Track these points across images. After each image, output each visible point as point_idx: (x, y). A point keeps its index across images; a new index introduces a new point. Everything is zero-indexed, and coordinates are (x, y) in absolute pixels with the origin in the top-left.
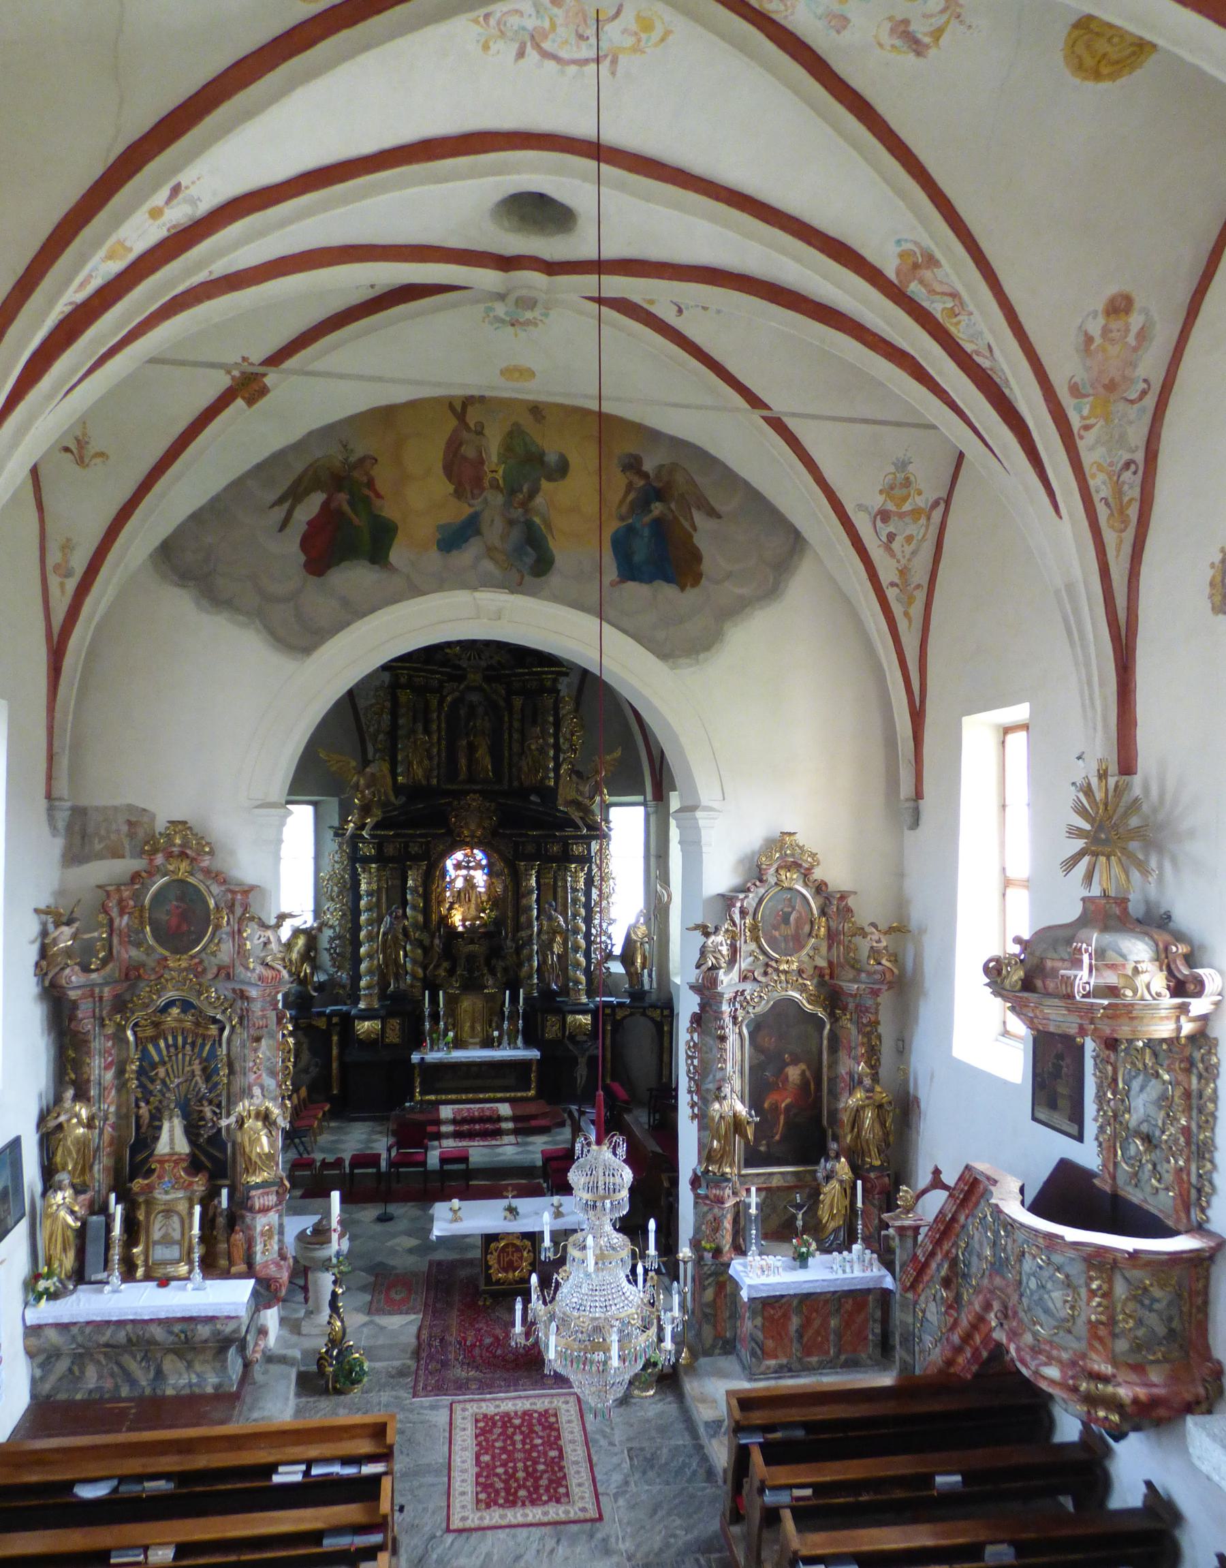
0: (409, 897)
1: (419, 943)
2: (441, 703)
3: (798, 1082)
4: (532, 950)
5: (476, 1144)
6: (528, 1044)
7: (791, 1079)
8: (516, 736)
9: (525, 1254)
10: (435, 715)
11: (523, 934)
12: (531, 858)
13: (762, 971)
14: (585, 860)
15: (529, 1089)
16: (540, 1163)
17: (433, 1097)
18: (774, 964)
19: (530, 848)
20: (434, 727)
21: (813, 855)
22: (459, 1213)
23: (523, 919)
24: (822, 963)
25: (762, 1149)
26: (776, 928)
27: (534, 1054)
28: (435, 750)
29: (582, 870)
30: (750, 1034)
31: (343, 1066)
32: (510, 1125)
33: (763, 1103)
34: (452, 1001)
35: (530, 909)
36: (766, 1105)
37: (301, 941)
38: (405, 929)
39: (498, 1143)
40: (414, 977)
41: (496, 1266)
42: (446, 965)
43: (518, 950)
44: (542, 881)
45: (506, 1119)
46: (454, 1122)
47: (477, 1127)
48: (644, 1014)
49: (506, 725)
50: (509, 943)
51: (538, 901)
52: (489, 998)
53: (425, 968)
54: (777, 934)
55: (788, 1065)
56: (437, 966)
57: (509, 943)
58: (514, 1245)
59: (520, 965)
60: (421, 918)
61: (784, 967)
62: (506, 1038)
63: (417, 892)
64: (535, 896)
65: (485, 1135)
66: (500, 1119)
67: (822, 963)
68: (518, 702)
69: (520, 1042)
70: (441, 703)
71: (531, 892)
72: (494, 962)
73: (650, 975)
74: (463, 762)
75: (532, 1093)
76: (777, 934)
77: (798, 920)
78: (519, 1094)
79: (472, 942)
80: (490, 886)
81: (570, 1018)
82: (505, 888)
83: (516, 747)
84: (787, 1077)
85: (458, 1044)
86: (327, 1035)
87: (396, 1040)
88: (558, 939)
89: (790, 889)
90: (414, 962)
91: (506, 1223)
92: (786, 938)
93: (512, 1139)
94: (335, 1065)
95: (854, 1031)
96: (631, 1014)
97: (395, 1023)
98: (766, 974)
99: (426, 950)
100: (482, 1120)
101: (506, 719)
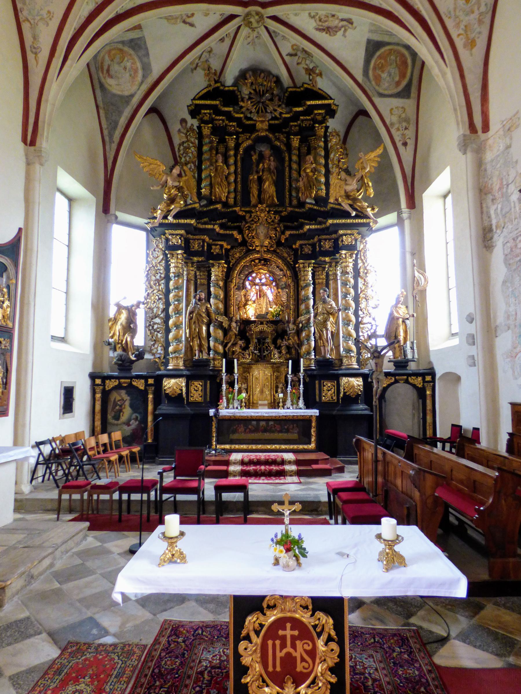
0: (212, 289)
1: (220, 326)
2: (237, 146)
4: (310, 332)
5: (261, 481)
6: (308, 406)
8: (295, 166)
9: (320, 643)
10: (232, 153)
11: (302, 318)
12: (308, 257)
14: (351, 248)
15: (310, 443)
16: (324, 498)
17: (227, 447)
19: (307, 250)
20: (232, 161)
22: (181, 545)
23: (303, 307)
27: (315, 412)
28: (232, 179)
29: (351, 257)
31: (155, 417)
32: (294, 468)
34: (246, 369)
35: (308, 298)
37: (124, 316)
38: (207, 309)
39: (282, 481)
40: (216, 352)
41: (258, 668)
42: (240, 342)
43: (298, 332)
44: (317, 281)
45: (290, 463)
46: (242, 463)
47: (263, 468)
48: (407, 382)
49: (287, 164)
50: (291, 326)
51: (314, 293)
52: (276, 368)
53: (225, 346)
56: (234, 345)
57: (291, 326)
58: (297, 624)
59: (300, 345)
60: (221, 306)
62: (289, 399)
63: (218, 285)
64: (311, 289)
65: (269, 475)
66: (283, 462)
68: (295, 142)
69: (301, 403)
70: (237, 146)
71: (307, 285)
72: (279, 341)
73: (412, 348)
74: (255, 191)
75: (312, 446)
78: (301, 447)
79: (262, 323)
80: (277, 296)
81: (344, 380)
82: (288, 297)
83: (295, 175)
85: (249, 404)
86: (144, 393)
87: (200, 399)
88: (331, 319)
90: (216, 340)
91: (278, 573)
93: (295, 479)
94: (150, 418)
96: (396, 382)
97: (197, 385)
99: (226, 332)
100: (267, 462)
101: (287, 159)
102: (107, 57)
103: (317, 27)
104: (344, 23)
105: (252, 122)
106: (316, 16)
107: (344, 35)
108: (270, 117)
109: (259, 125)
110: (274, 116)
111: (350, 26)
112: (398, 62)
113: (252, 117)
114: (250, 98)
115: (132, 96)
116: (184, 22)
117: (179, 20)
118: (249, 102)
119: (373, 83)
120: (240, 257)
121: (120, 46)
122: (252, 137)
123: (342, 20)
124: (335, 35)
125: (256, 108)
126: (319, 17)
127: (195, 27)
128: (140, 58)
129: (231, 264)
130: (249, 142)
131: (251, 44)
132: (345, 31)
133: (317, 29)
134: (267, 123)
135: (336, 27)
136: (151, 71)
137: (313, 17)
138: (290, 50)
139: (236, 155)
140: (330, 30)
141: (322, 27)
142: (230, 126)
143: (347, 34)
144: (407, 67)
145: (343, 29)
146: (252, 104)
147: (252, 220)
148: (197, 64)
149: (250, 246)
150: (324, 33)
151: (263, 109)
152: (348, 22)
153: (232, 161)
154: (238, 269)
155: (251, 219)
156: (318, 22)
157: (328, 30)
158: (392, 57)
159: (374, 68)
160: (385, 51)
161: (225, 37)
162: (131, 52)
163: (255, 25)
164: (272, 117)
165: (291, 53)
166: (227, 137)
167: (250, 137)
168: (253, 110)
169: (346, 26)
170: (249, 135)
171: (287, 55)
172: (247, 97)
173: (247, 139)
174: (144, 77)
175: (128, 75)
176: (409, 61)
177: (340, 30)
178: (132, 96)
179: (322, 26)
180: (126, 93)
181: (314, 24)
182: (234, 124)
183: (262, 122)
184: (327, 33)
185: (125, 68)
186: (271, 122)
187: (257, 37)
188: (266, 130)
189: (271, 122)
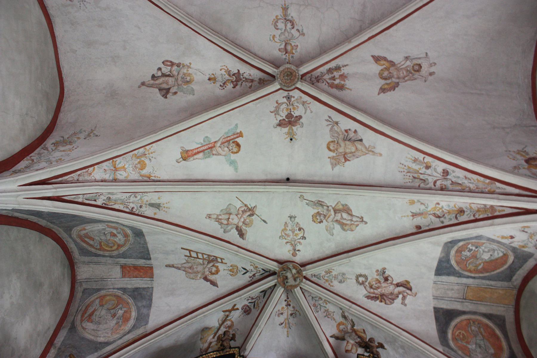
102: (97, 301)
103: (368, 294)
104: (401, 289)
106: (366, 282)
107: (403, 303)
111: (408, 291)
112: (484, 333)
115: (107, 344)
116: (206, 279)
117: (199, 276)
119: (460, 353)
121: (119, 293)
123: (398, 285)
124: (391, 303)
126: (369, 283)
127: (218, 287)
128: (138, 309)
131: (284, 325)
132: (404, 298)
133: (368, 297)
135: (392, 294)
136: (147, 323)
137: (363, 283)
138: (335, 331)
140: (384, 297)
141: (374, 295)
143: (406, 302)
144: (498, 338)
145: (401, 296)
148: (211, 343)
150: (378, 302)
152: (404, 287)
156: (368, 289)
157: (382, 298)
158: (473, 328)
159: (454, 339)
160: (461, 321)
161: (252, 308)
162: (131, 301)
163: (291, 282)
165: (336, 335)
169: (404, 292)
171: (331, 337)
174: (134, 327)
175: (114, 322)
176: (498, 332)
177: (398, 297)
178: (107, 344)
179: (374, 293)
180: (101, 339)
181: (365, 292)
184: (381, 301)
185: (114, 316)
187: (291, 315)
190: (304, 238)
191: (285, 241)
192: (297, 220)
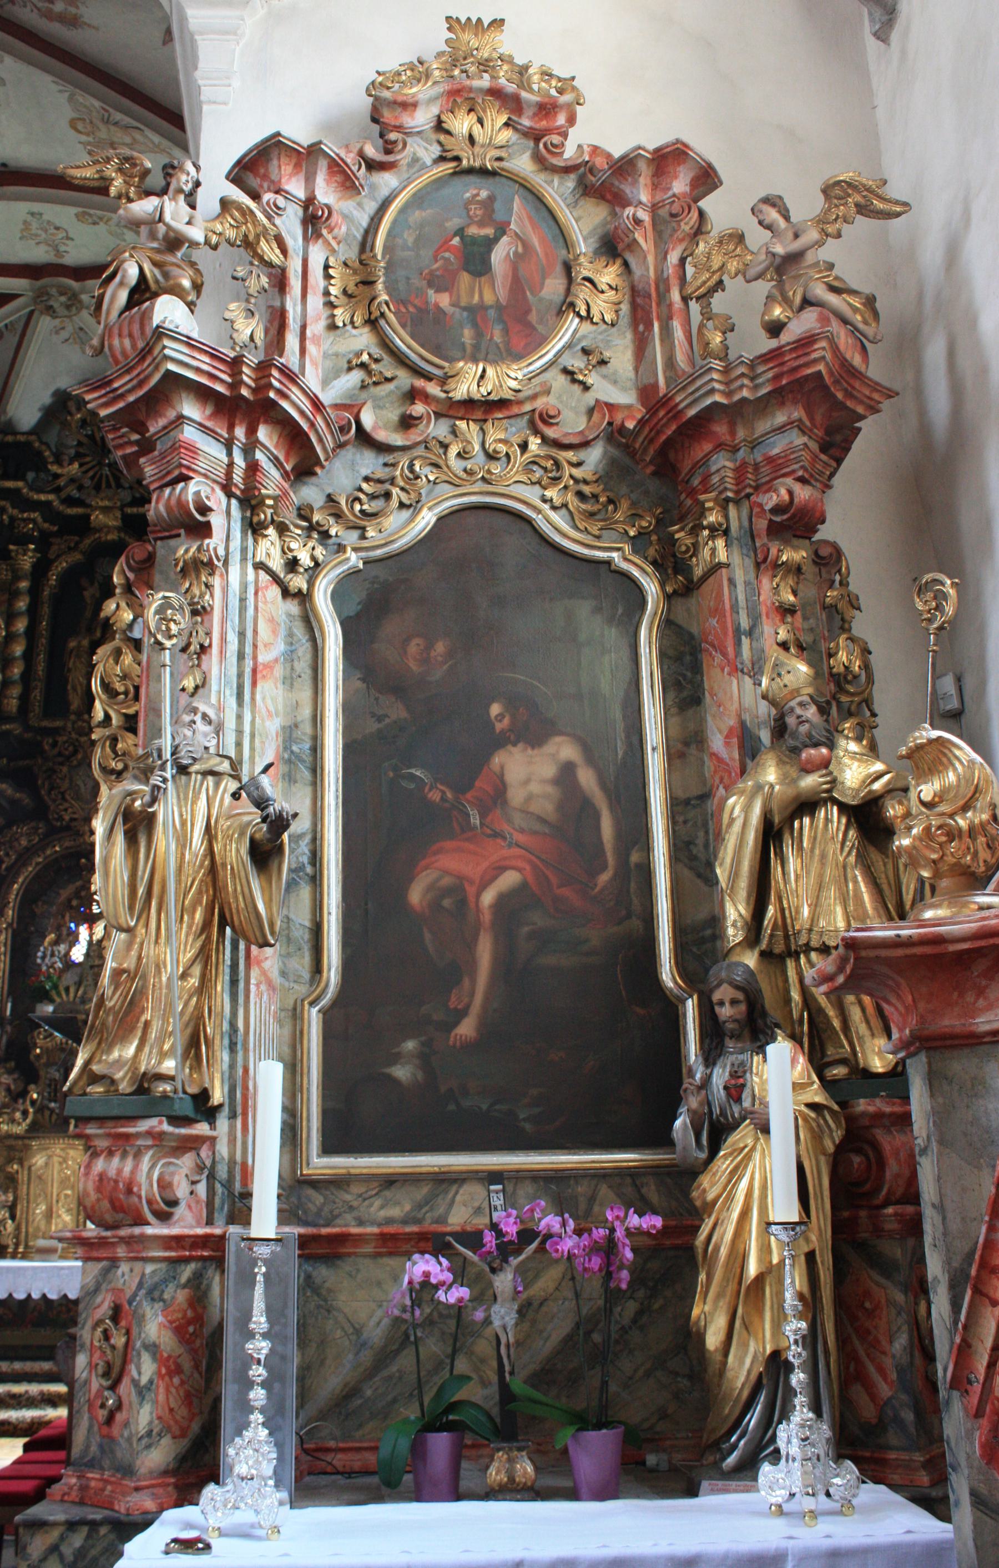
2: (40, 570)
3: (546, 809)
7: (516, 796)
13: (393, 415)
18: (433, 389)
21: (567, 85)
24: (625, 397)
25: (402, 1072)
26: (440, 282)
30: (347, 625)
33: (402, 892)
36: (416, 895)
54: (444, 300)
55: (501, 742)
61: (464, 388)
67: (625, 397)
76: (444, 300)
77: (516, 262)
84: (500, 791)
89: (483, 172)
92: (476, 313)
95: (741, 570)
98: (407, 423)
105: (80, 510)
108: (129, 499)
109: (98, 518)
110: (138, 495)
113: (83, 497)
114: (78, 456)
118: (76, 465)
120: (27, 849)
122: (81, 546)
125: (92, 478)
129: (4, 866)
130: (77, 557)
134: (118, 514)
139: (34, 592)
142: (24, 520)
146: (84, 468)
147: (60, 754)
149: (57, 820)
151: (111, 479)
153: (22, 604)
154: (20, 880)
155: (56, 751)
164: (134, 497)
166: (12, 547)
167: (77, 544)
168: (87, 483)
170: (77, 538)
172: (72, 452)
173: (70, 549)
182: (35, 515)
183: (105, 510)
186: (129, 510)
188: (119, 529)
189: (129, 510)
190: (68, 238)
191: (33, 242)
192: (45, 217)
